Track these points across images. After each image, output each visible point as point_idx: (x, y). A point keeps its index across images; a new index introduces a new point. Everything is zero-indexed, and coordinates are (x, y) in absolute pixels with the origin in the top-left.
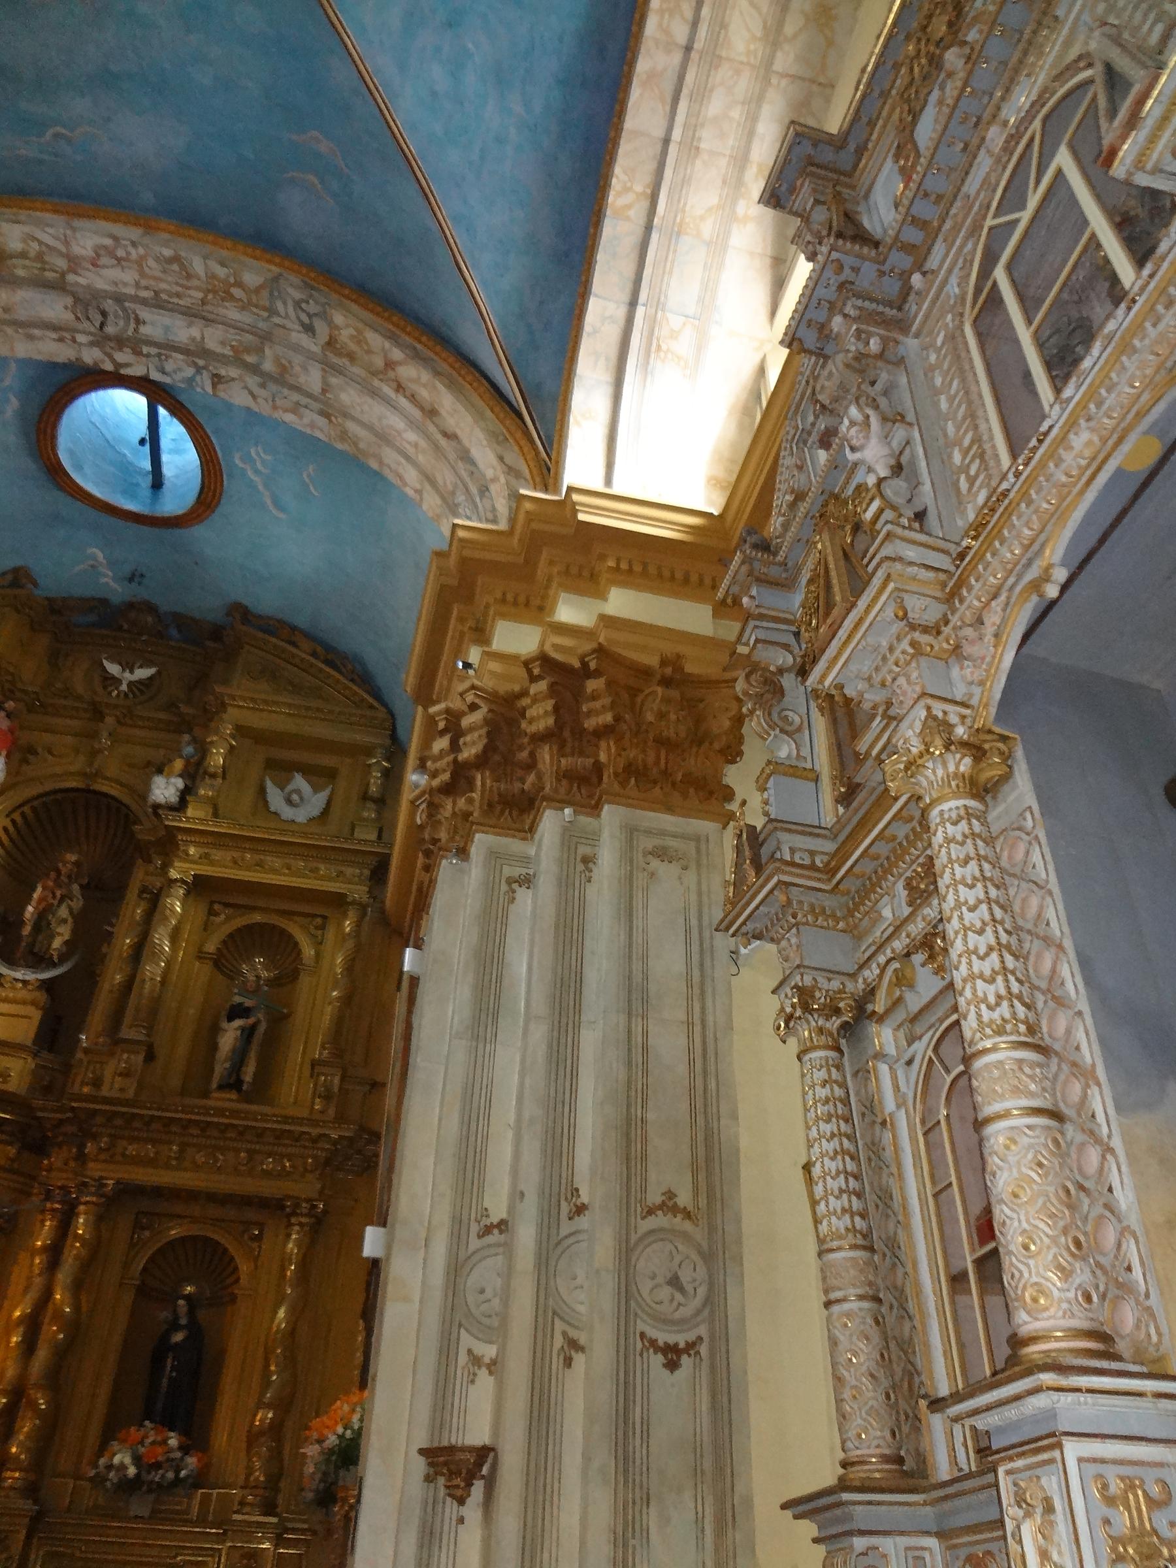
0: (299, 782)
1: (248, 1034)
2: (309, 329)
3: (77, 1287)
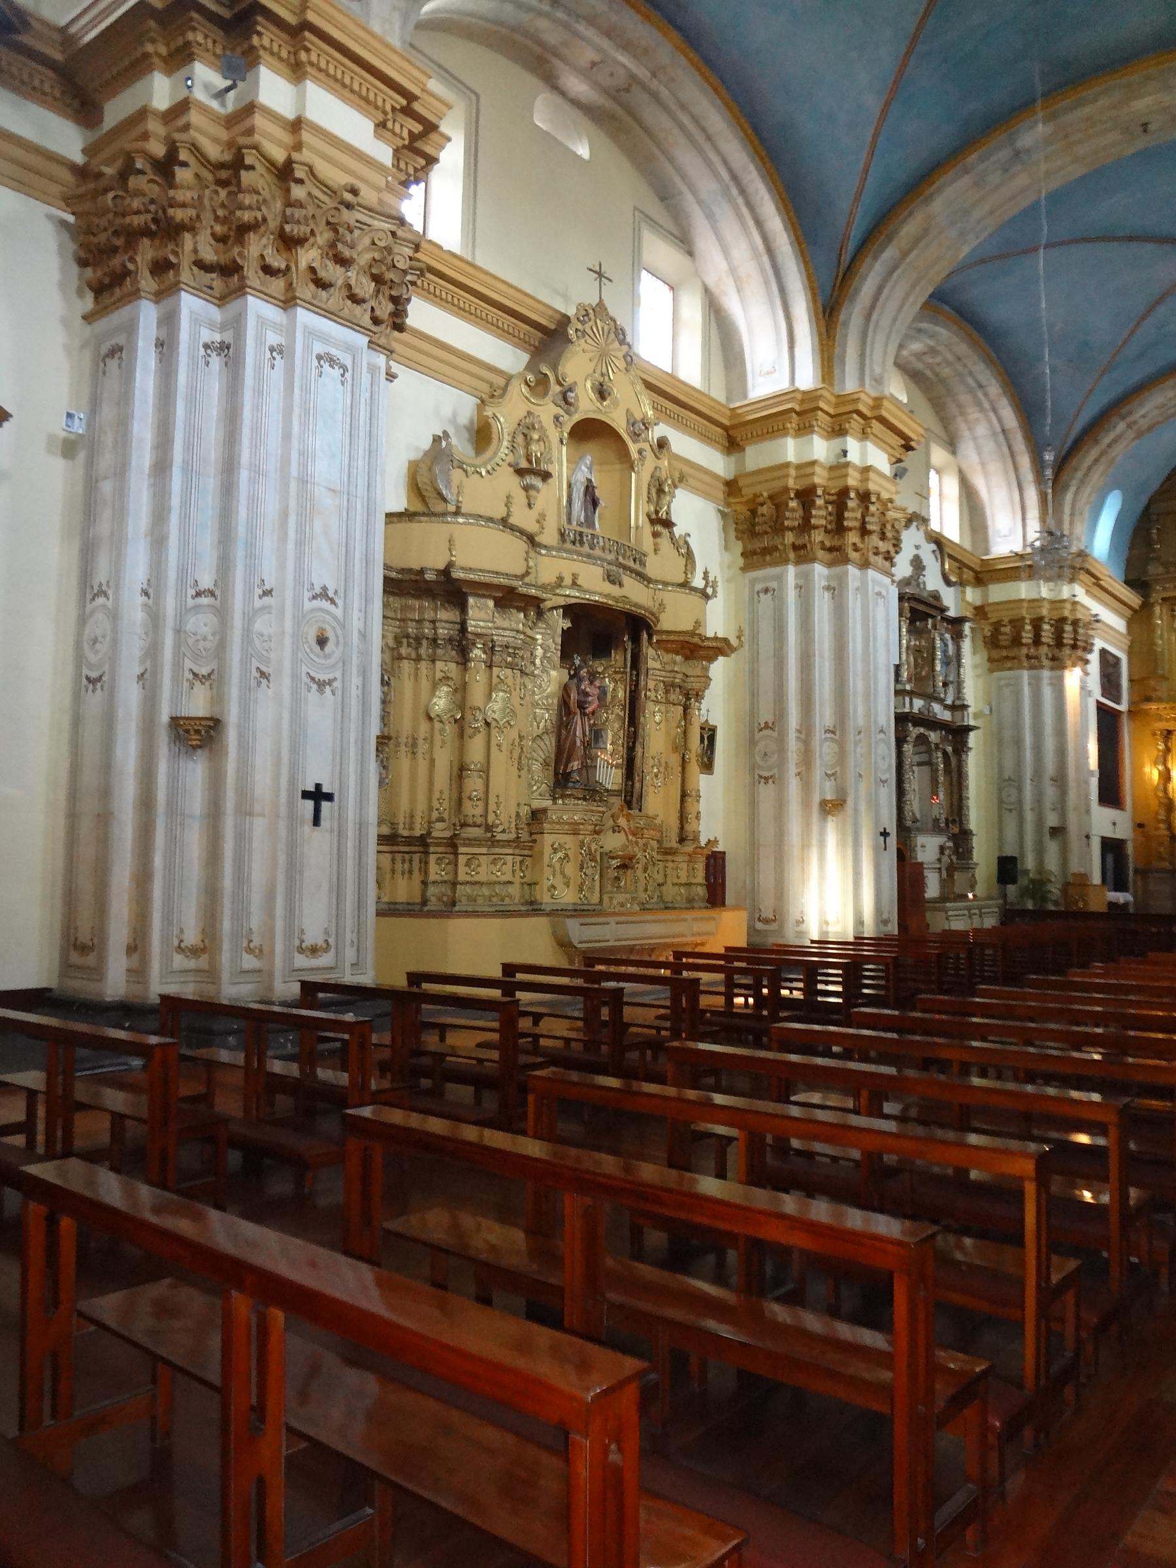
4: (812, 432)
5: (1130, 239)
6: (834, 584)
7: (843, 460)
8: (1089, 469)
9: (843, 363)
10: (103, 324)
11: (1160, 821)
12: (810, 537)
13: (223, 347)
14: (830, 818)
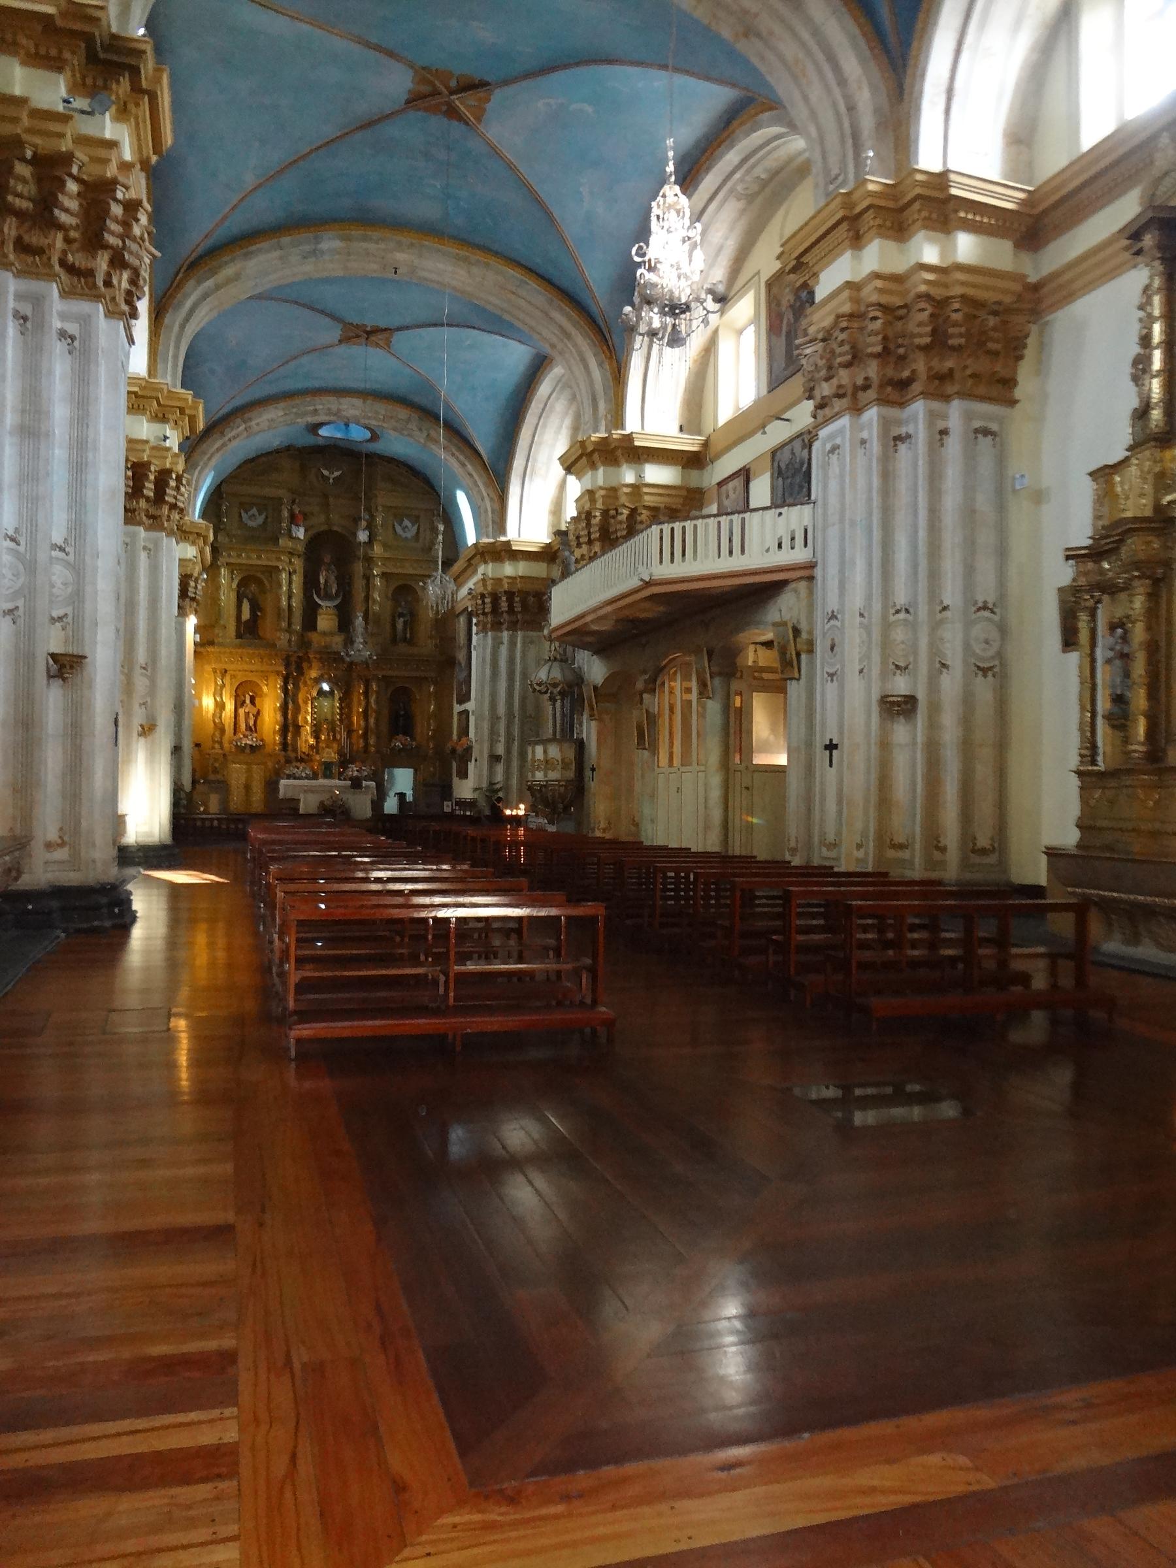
0: (406, 522)
1: (405, 623)
2: (420, 430)
3: (377, 702)
4: (143, 415)
5: (322, 312)
6: (151, 546)
7: (162, 443)
8: (212, 455)
9: (166, 361)
11: (214, 742)
12: (138, 503)
14: (142, 740)
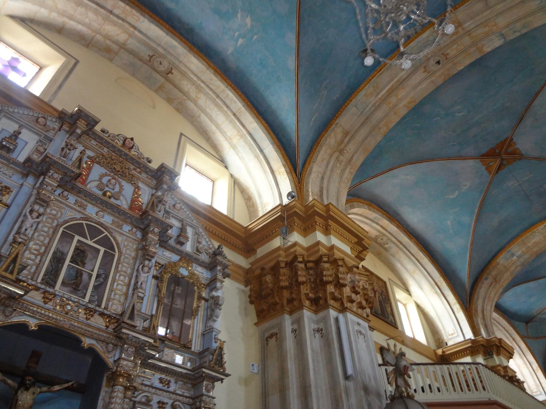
10: (266, 325)
13: (319, 330)
